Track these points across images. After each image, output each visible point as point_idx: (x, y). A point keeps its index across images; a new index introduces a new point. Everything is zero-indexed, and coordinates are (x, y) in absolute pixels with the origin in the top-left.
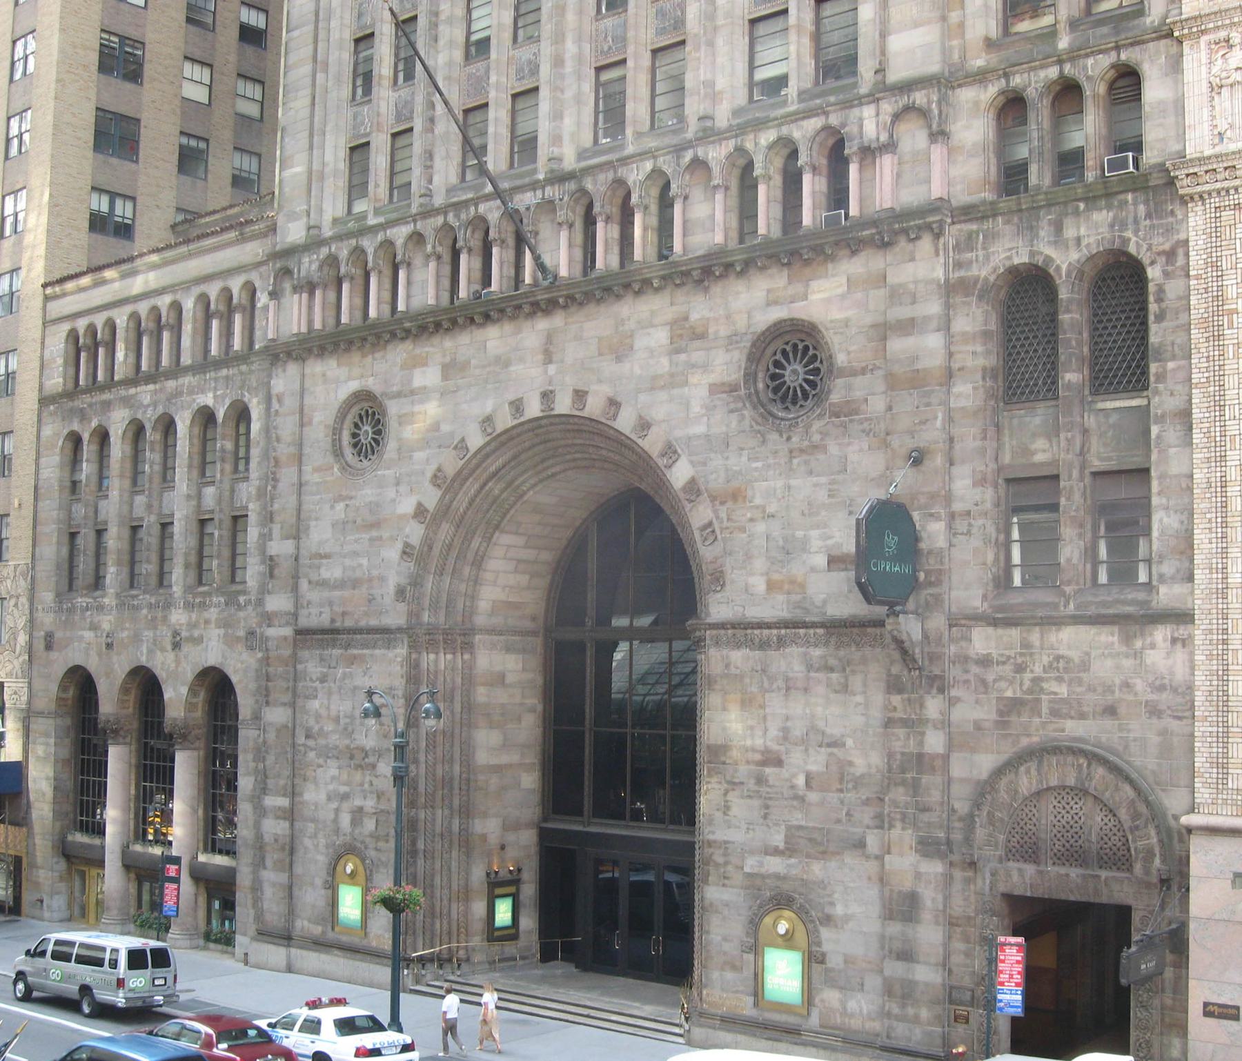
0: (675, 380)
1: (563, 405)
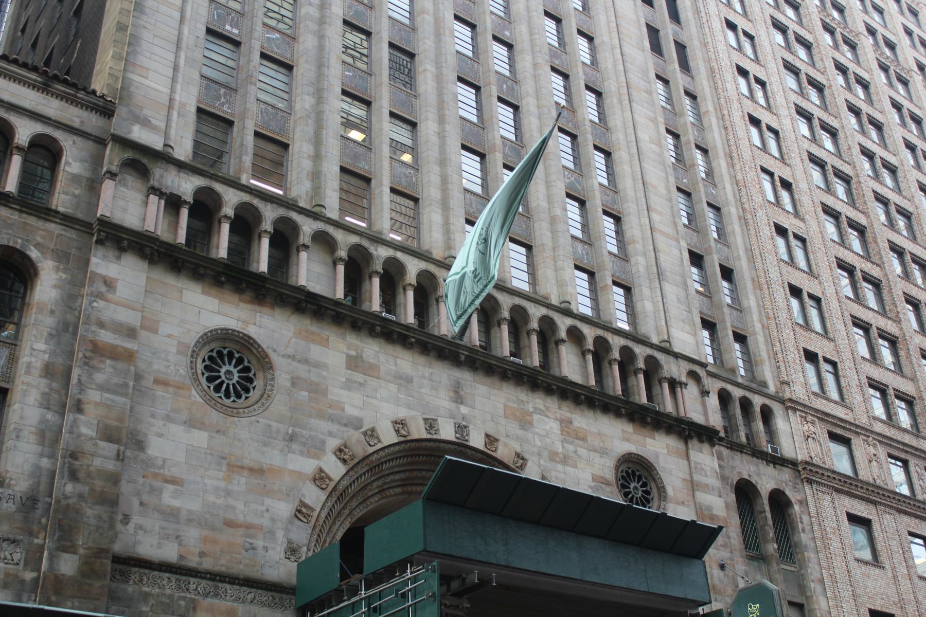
1: (477, 441)
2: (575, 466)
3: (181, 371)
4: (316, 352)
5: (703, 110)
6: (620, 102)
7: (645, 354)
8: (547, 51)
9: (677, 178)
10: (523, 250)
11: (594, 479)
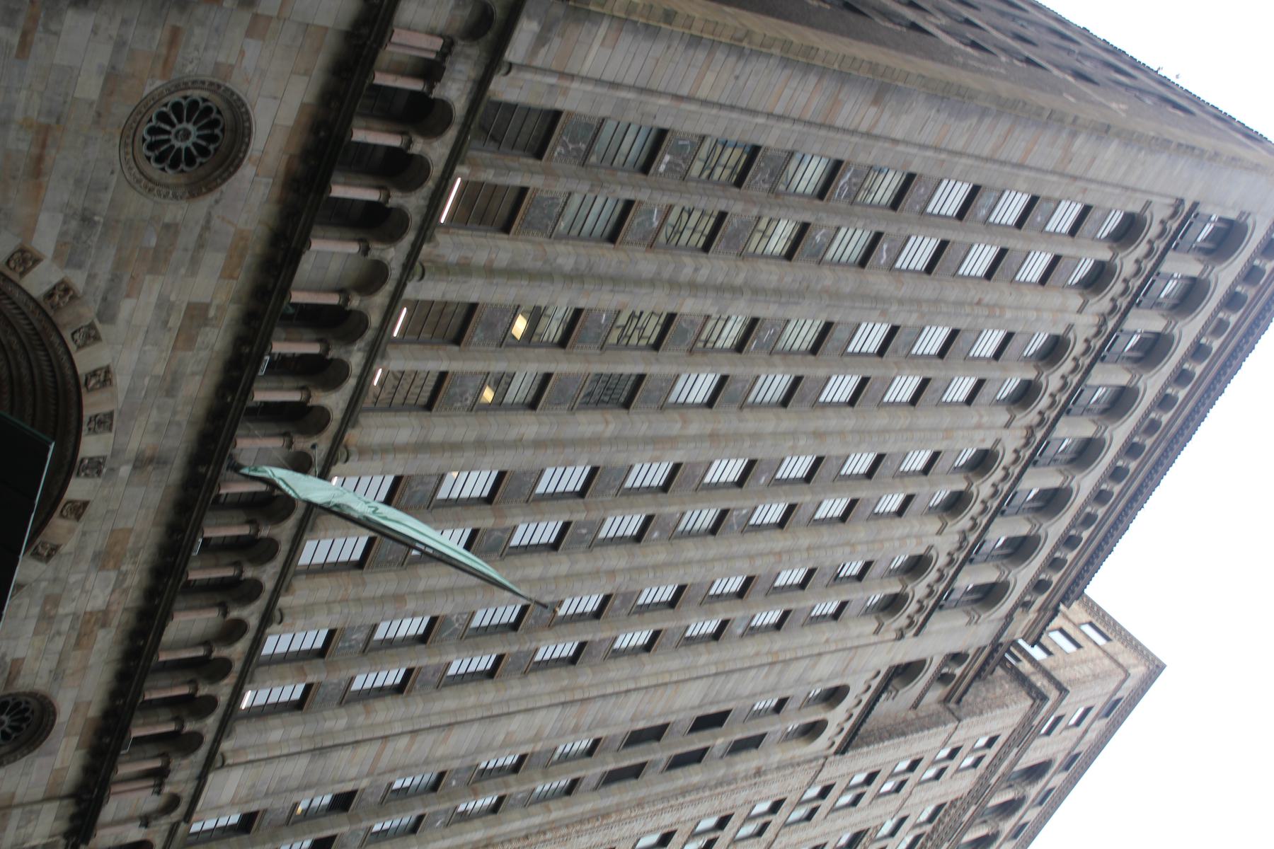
0: (46, 618)
1: (77, 489)
2: (36, 633)
3: (190, 68)
4: (214, 260)
5: (553, 804)
6: (563, 690)
7: (204, 731)
8: (631, 589)
9: (457, 771)
10: (357, 556)
11: (17, 660)
